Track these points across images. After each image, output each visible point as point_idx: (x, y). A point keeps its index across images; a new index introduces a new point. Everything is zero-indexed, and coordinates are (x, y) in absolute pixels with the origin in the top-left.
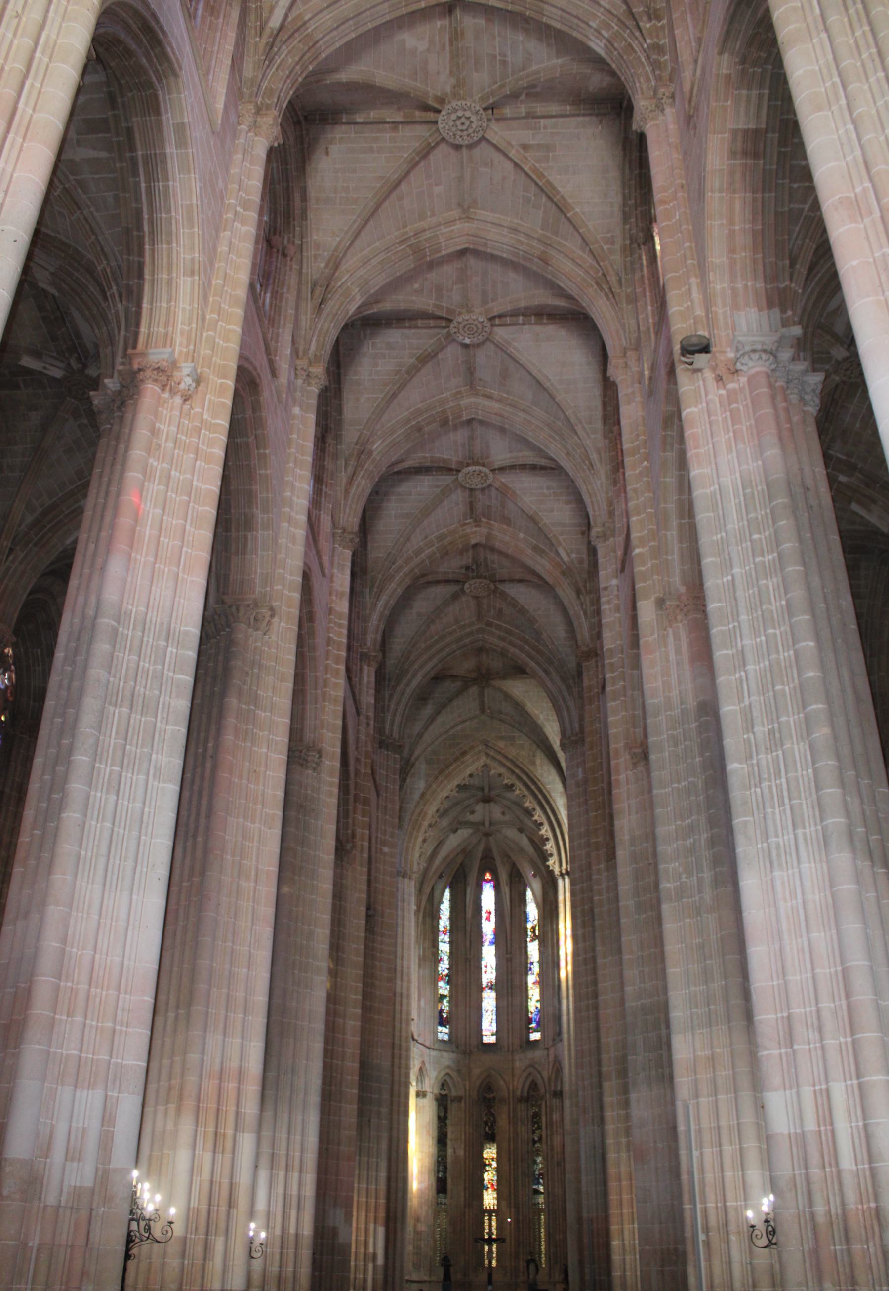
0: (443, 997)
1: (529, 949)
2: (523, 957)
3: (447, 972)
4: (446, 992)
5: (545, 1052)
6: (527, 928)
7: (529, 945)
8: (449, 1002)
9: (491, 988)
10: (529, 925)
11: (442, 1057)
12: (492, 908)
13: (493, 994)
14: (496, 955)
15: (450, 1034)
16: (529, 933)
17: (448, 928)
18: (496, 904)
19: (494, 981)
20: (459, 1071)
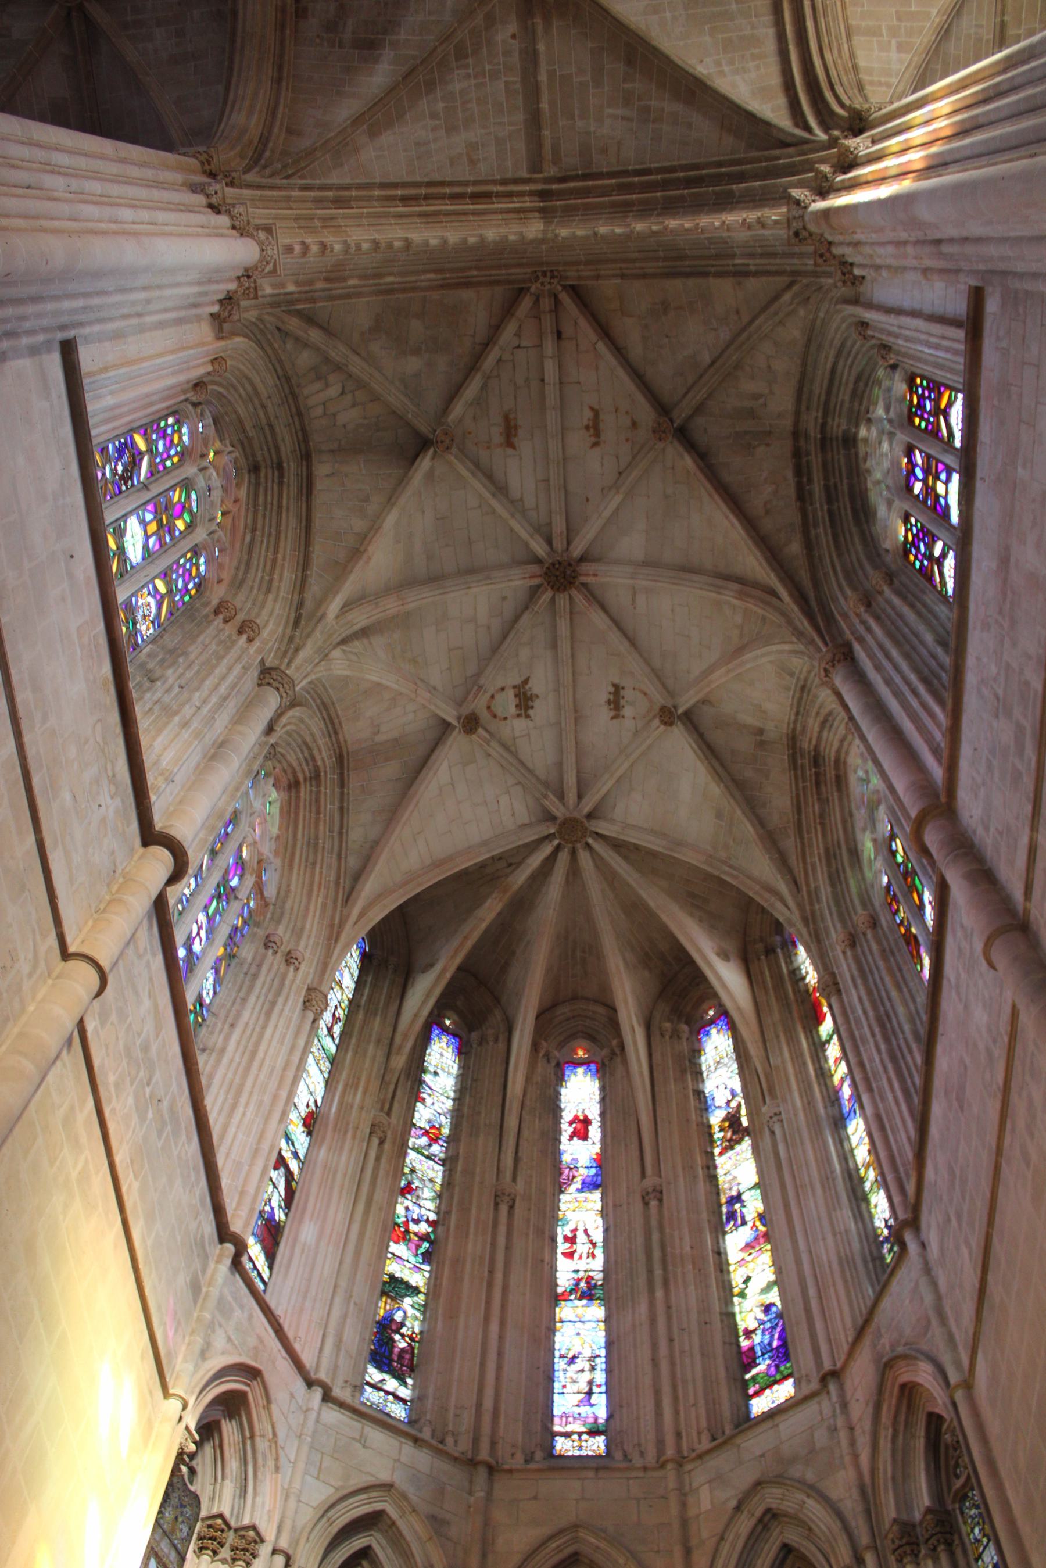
0: (396, 1288)
1: (720, 1171)
2: (702, 1187)
3: (424, 1228)
4: (418, 1279)
5: (826, 1405)
6: (710, 1127)
7: (719, 1161)
8: (424, 1308)
9: (588, 1295)
10: (716, 1118)
11: (362, 1440)
12: (594, 1112)
13: (597, 1311)
14: (603, 1213)
15: (414, 1405)
16: (718, 1135)
17: (446, 1131)
18: (603, 1101)
19: (599, 1276)
20: (437, 1523)
